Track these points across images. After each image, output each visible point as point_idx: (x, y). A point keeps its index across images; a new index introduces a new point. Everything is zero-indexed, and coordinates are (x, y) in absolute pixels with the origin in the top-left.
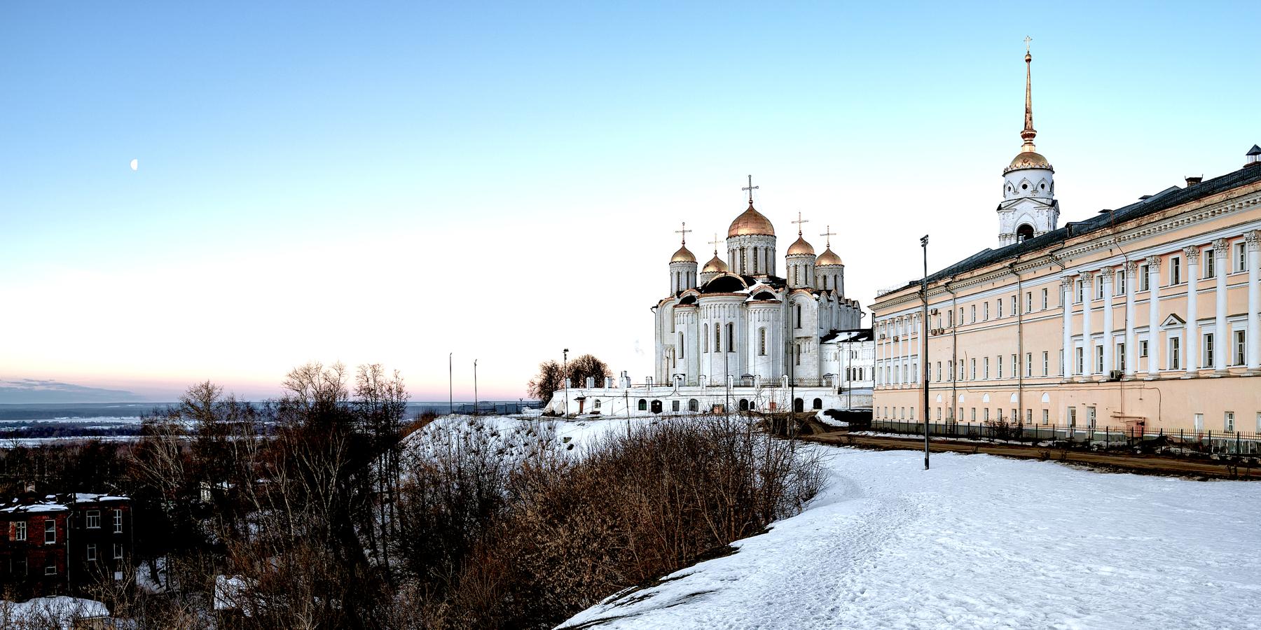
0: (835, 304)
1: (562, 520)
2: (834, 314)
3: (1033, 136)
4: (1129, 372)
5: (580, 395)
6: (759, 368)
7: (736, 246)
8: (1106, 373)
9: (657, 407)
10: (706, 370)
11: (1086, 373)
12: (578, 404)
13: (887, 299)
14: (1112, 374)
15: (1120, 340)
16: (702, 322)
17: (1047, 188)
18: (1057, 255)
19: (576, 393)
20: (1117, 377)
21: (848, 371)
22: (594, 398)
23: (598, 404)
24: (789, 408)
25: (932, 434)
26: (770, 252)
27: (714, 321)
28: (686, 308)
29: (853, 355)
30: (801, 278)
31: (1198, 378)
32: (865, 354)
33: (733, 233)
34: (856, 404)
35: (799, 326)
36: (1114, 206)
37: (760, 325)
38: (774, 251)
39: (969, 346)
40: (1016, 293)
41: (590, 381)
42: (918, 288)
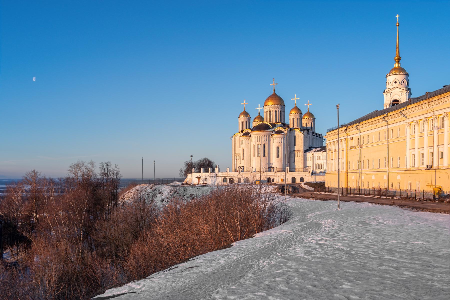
0: (311, 135)
1: (173, 231)
2: (311, 140)
4: (435, 165)
5: (198, 176)
6: (277, 163)
8: (425, 166)
9: (231, 181)
10: (253, 165)
11: (416, 166)
12: (197, 180)
14: (427, 166)
16: (252, 143)
18: (403, 112)
20: (429, 168)
22: (204, 177)
23: (206, 179)
24: (289, 181)
25: (348, 193)
28: (245, 137)
31: (448, 169)
34: (319, 179)
37: (277, 145)
38: (284, 112)
40: (386, 130)
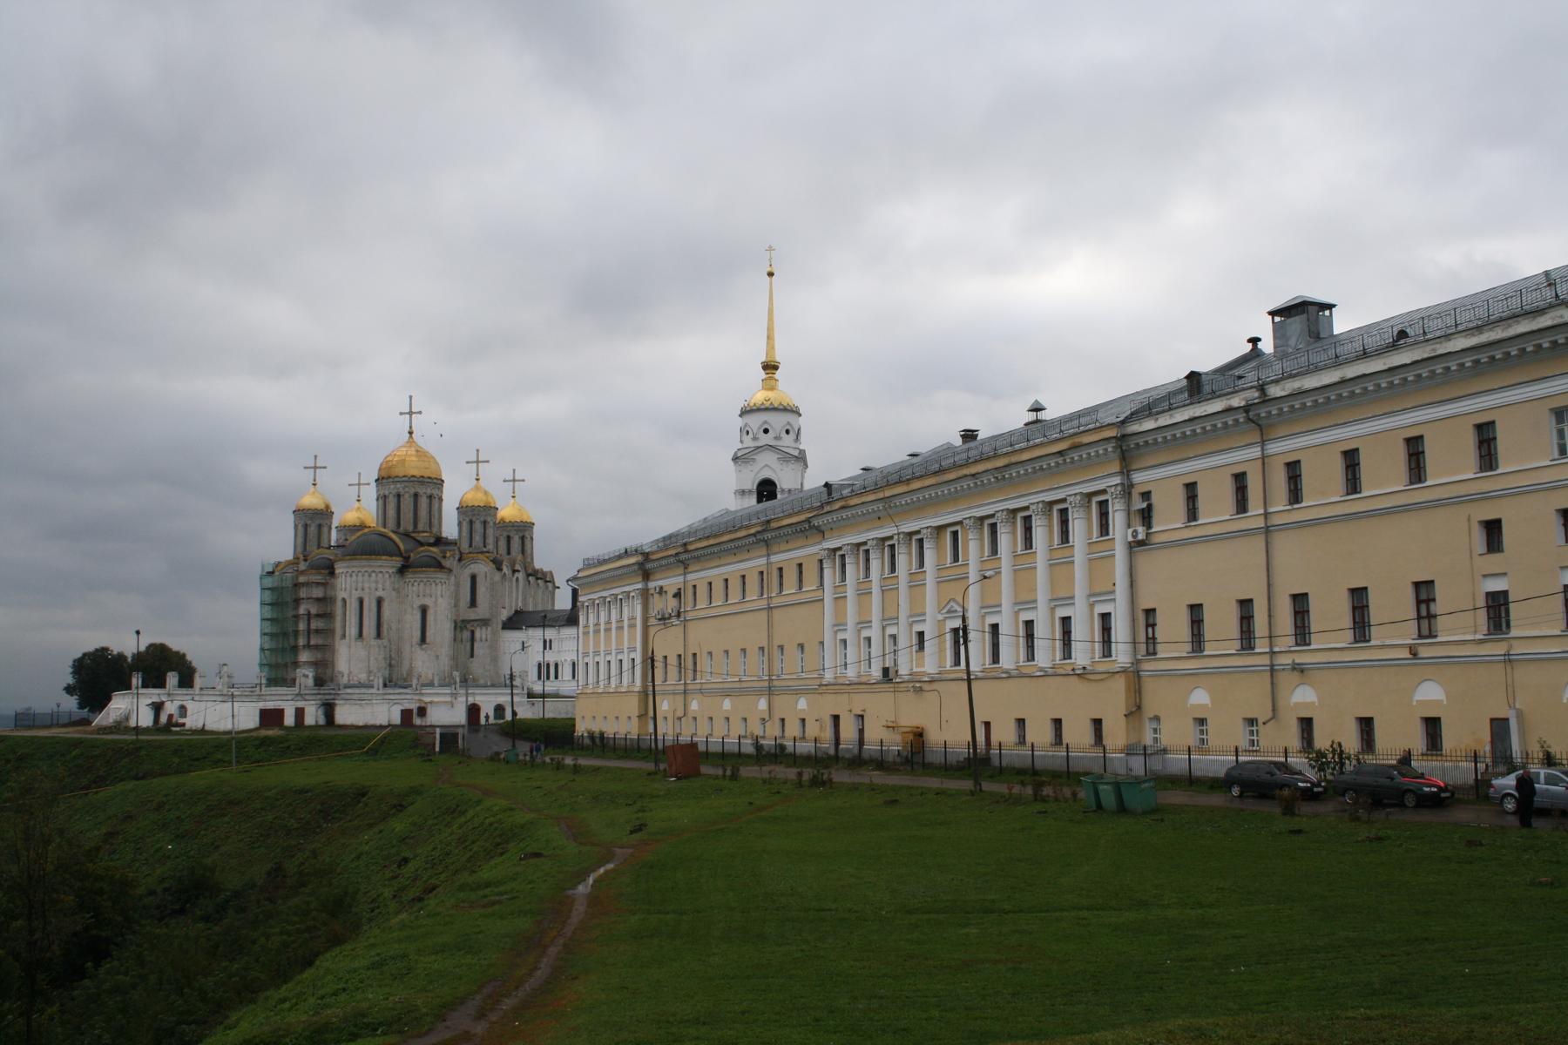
0: (521, 575)
3: (776, 368)
5: (156, 699)
7: (391, 489)
8: (876, 673)
13: (600, 574)
15: (891, 630)
17: (792, 436)
19: (154, 694)
23: (183, 710)
26: (435, 500)
27: (356, 594)
29: (547, 644)
30: (477, 538)
32: (566, 645)
33: (384, 474)
34: (553, 710)
35: (473, 603)
36: (877, 464)
38: (441, 499)
39: (703, 636)
41: (172, 679)
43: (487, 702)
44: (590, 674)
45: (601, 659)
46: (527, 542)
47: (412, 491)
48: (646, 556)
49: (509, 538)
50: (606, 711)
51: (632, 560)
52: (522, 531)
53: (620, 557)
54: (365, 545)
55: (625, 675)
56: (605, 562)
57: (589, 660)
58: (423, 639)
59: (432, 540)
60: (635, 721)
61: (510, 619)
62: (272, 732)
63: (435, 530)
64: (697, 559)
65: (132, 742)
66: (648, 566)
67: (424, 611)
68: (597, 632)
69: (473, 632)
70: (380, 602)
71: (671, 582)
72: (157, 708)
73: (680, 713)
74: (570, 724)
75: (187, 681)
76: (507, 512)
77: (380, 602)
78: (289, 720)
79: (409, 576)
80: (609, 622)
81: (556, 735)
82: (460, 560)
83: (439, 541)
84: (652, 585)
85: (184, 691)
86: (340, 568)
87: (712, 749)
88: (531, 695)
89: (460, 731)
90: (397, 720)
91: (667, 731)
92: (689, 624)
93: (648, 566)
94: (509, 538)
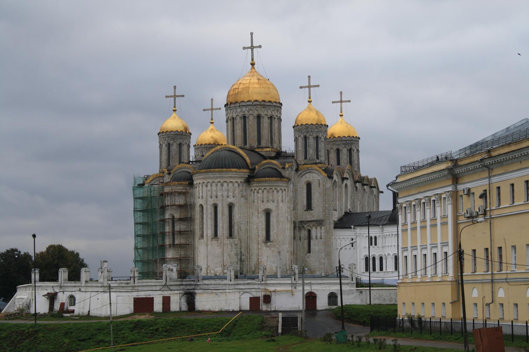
0: (349, 182)
5: (51, 291)
13: (414, 179)
19: (49, 287)
21: (367, 259)
22: (67, 294)
23: (72, 299)
26: (275, 120)
27: (211, 202)
30: (311, 152)
32: (387, 242)
34: (378, 297)
35: (309, 207)
38: (280, 119)
41: (63, 274)
42: (449, 164)
43: (322, 291)
44: (409, 265)
45: (418, 253)
46: (354, 154)
47: (256, 113)
48: (455, 162)
49: (338, 151)
50: (424, 299)
51: (443, 166)
52: (350, 144)
53: (432, 164)
54: (217, 161)
55: (439, 264)
56: (419, 168)
57: (408, 253)
58: (268, 238)
59: (273, 154)
60: (449, 307)
61: (341, 220)
62: (143, 317)
63: (275, 146)
64: (501, 164)
65: (32, 326)
66: (457, 171)
67: (268, 214)
68: (414, 229)
69: (309, 231)
70: (231, 207)
71: (477, 184)
72: (52, 297)
73: (488, 300)
74: (393, 309)
75: (74, 277)
76: (337, 128)
77: (231, 207)
78: (158, 307)
79: (255, 185)
80: (424, 221)
81: (382, 320)
82: (297, 170)
83: (279, 155)
84: (460, 187)
85: (73, 284)
86: (197, 181)
87: (517, 332)
88: (359, 284)
89: (299, 316)
90: (246, 306)
91: (474, 315)
92: (496, 222)
93: (457, 171)
94: (338, 151)
